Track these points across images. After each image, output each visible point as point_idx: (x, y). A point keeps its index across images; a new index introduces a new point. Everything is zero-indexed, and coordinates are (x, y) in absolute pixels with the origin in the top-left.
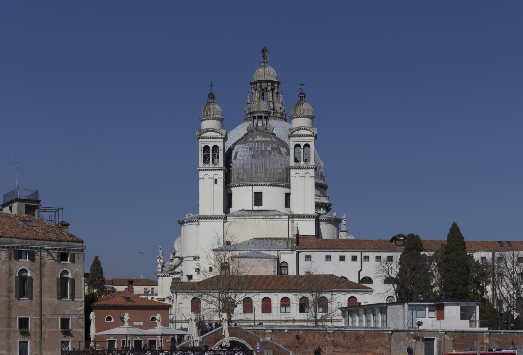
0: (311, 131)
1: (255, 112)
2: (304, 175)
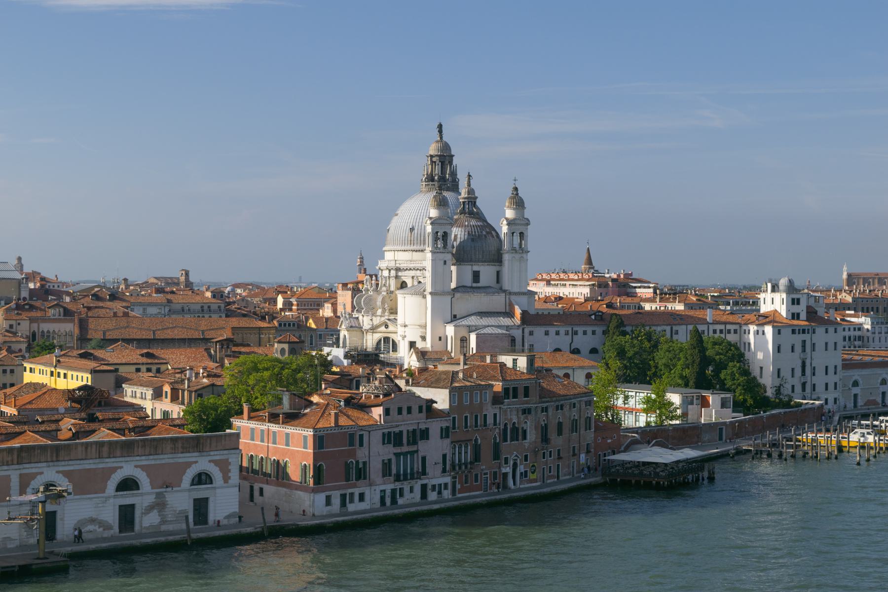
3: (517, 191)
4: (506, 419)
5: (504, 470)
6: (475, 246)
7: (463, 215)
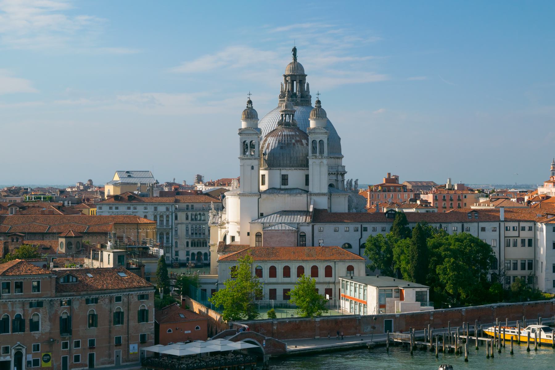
3: (320, 104)
6: (283, 153)
7: (280, 126)
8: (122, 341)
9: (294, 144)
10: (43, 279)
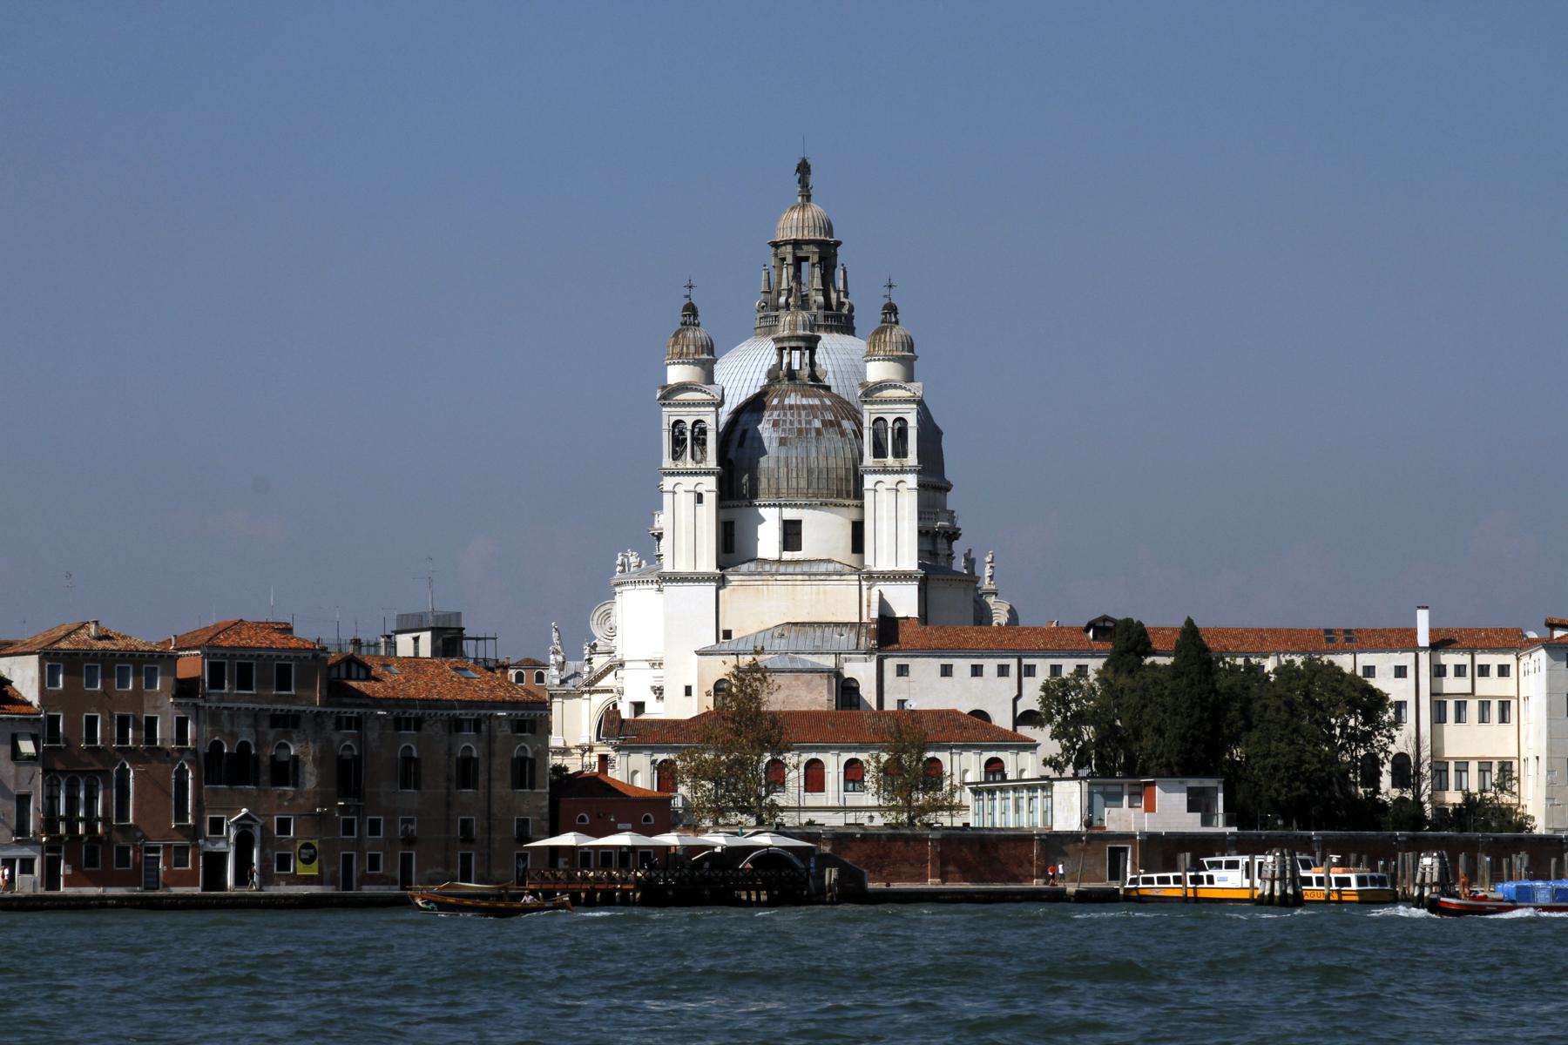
0: (910, 390)
1: (784, 337)
2: (894, 487)
3: (896, 314)
4: (213, 733)
5: (210, 847)
8: (476, 831)
9: (818, 432)
10: (301, 660)
